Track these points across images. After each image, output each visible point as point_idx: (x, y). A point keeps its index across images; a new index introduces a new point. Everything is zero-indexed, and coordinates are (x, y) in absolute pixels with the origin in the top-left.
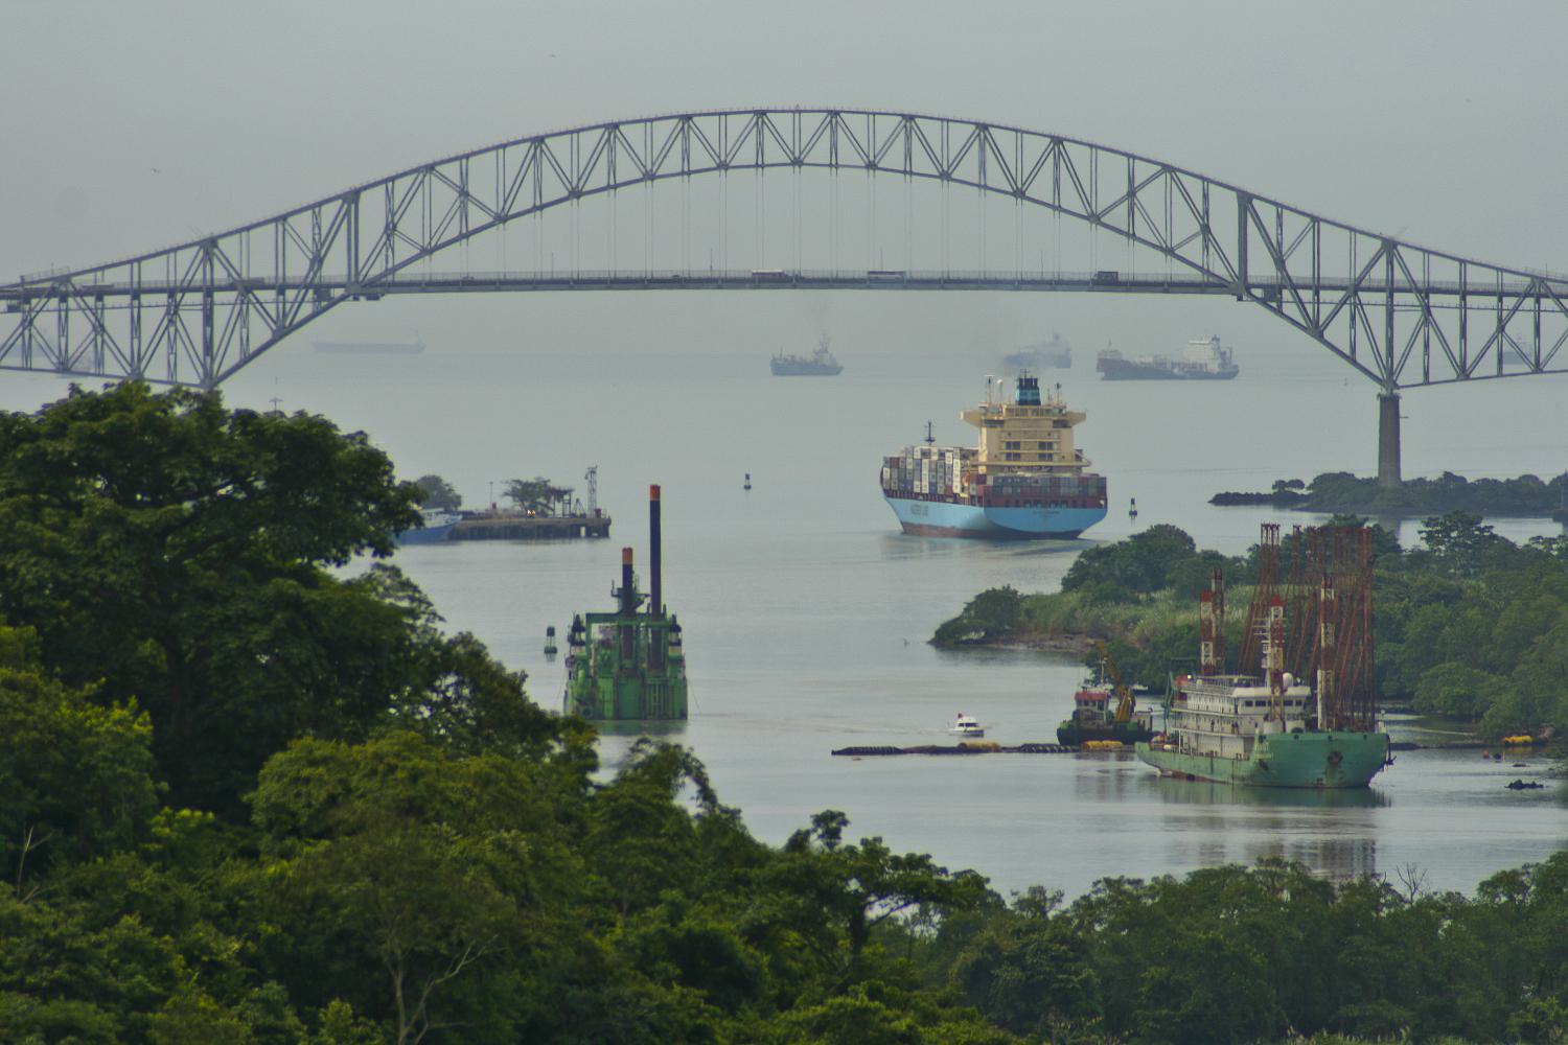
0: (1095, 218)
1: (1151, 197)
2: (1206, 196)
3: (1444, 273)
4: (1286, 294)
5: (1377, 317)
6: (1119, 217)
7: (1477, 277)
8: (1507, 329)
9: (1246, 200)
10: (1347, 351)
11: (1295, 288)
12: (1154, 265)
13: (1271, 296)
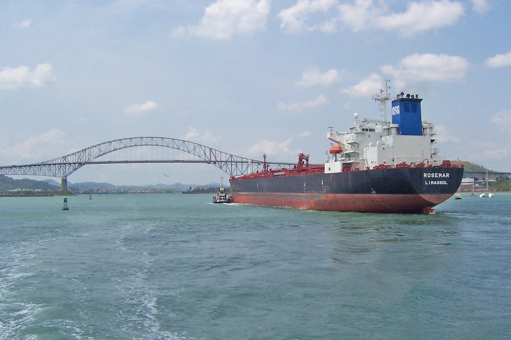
0: (189, 152)
3: (239, 160)
4: (217, 163)
5: (230, 166)
6: (193, 152)
7: (244, 160)
9: (211, 149)
10: (225, 171)
11: (218, 162)
12: (197, 159)
13: (215, 162)
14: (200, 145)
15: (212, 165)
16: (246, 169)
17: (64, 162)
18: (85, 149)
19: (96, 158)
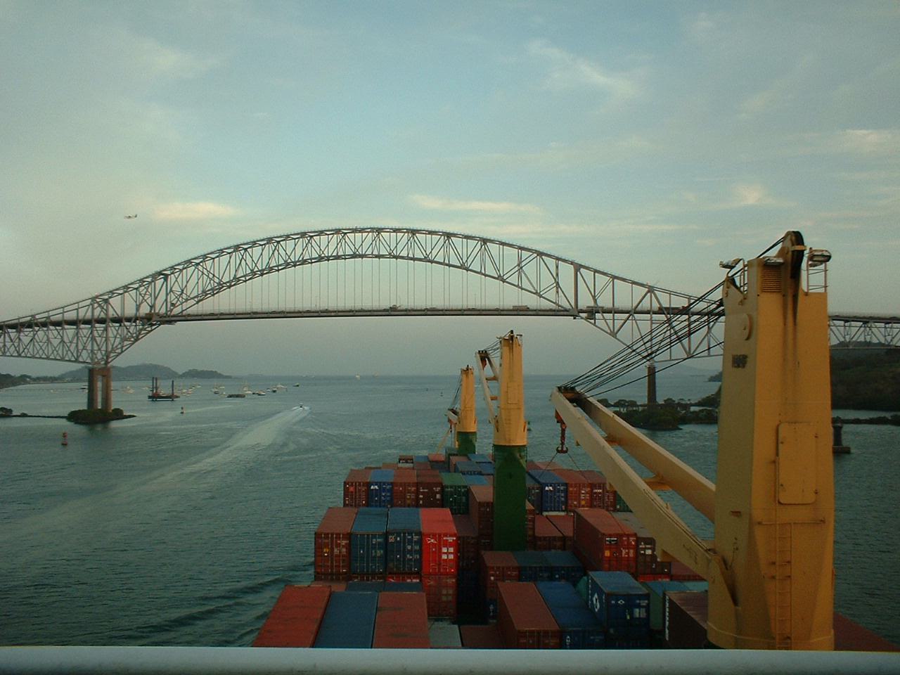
0: (501, 278)
1: (530, 269)
2: (557, 267)
6: (514, 279)
8: (713, 331)
9: (578, 267)
14: (540, 254)
15: (581, 323)
16: (704, 338)
17: (103, 315)
18: (160, 273)
19: (198, 302)
